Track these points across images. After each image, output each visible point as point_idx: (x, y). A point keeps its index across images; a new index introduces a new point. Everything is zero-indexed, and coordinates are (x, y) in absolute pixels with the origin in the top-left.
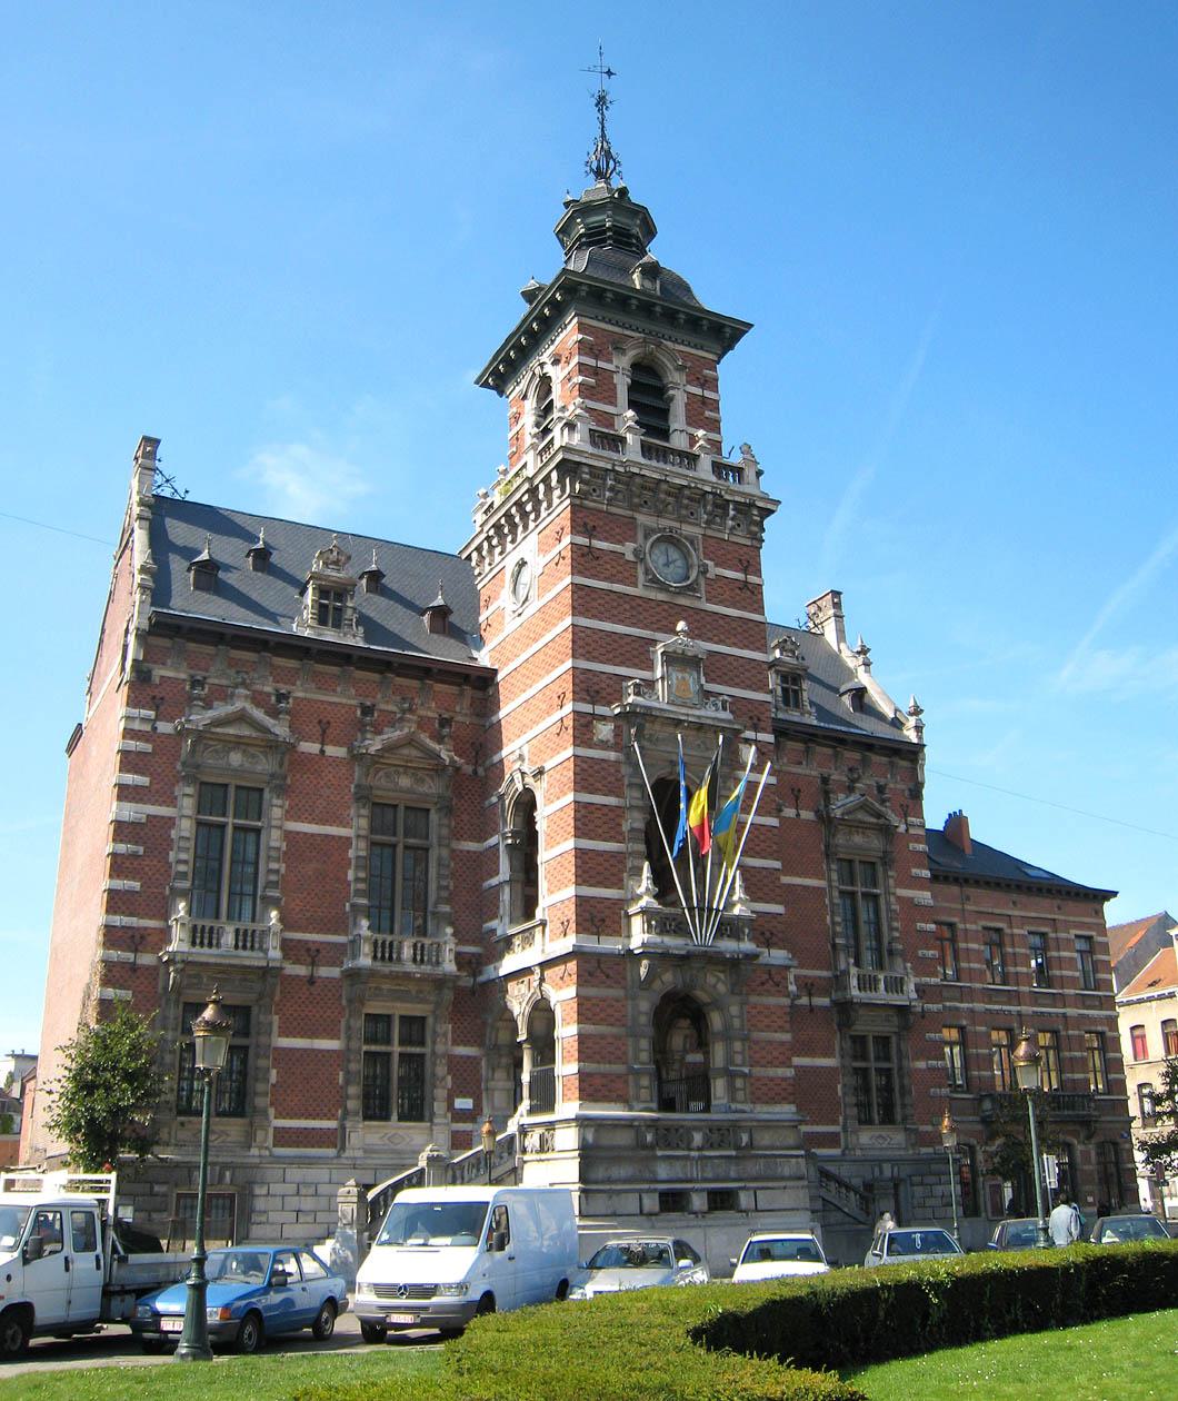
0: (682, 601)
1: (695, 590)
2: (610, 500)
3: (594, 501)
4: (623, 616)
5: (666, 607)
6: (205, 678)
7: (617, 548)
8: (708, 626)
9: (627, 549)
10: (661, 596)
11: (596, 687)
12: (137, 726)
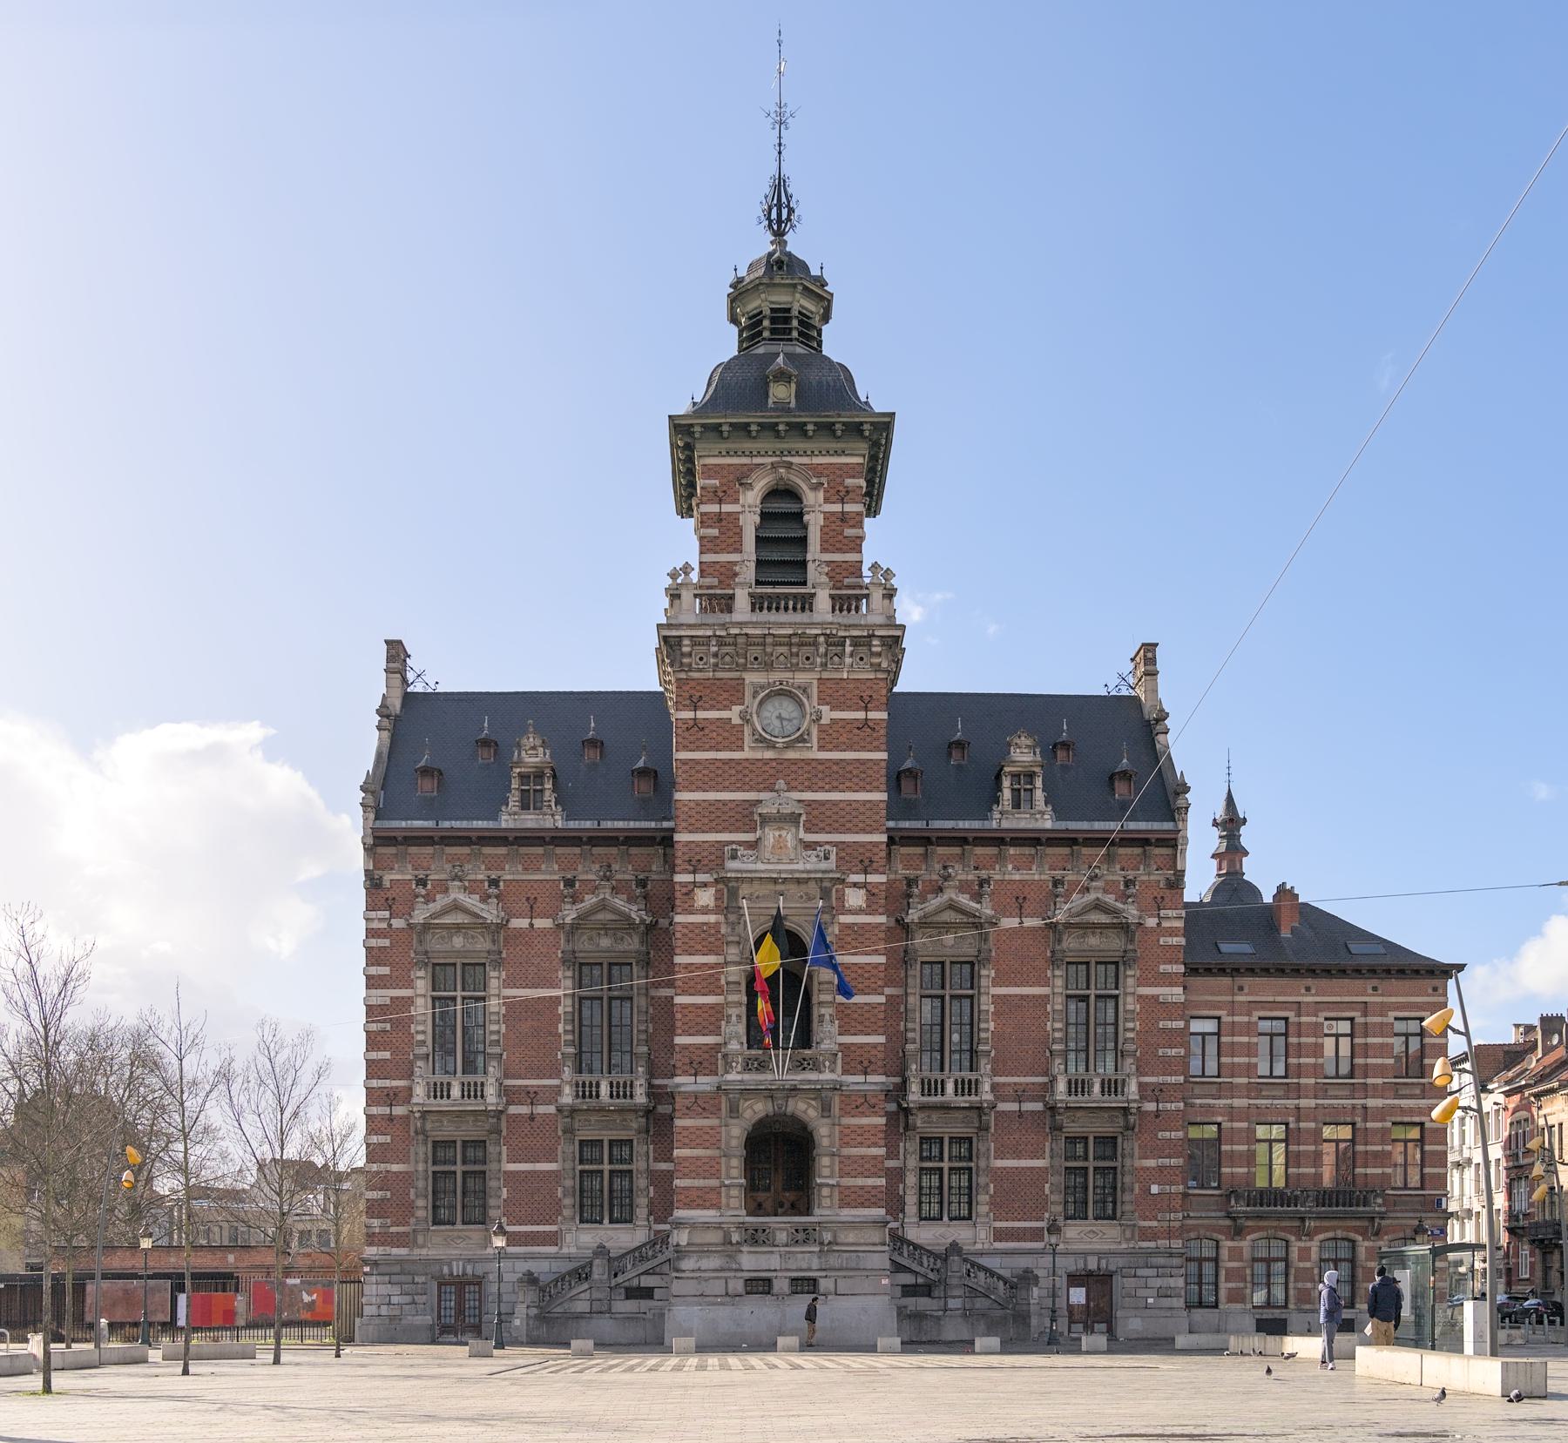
0: (791, 755)
1: (804, 741)
2: (716, 665)
3: (700, 670)
4: (727, 783)
5: (774, 764)
6: (427, 876)
7: (724, 714)
8: (820, 775)
9: (734, 714)
10: (769, 754)
11: (698, 857)
12: (375, 925)
